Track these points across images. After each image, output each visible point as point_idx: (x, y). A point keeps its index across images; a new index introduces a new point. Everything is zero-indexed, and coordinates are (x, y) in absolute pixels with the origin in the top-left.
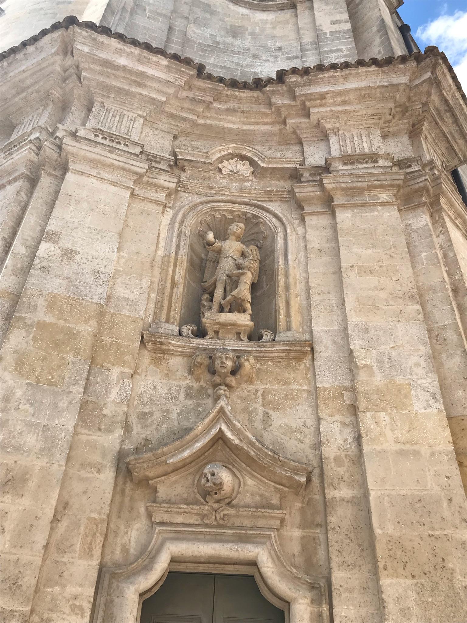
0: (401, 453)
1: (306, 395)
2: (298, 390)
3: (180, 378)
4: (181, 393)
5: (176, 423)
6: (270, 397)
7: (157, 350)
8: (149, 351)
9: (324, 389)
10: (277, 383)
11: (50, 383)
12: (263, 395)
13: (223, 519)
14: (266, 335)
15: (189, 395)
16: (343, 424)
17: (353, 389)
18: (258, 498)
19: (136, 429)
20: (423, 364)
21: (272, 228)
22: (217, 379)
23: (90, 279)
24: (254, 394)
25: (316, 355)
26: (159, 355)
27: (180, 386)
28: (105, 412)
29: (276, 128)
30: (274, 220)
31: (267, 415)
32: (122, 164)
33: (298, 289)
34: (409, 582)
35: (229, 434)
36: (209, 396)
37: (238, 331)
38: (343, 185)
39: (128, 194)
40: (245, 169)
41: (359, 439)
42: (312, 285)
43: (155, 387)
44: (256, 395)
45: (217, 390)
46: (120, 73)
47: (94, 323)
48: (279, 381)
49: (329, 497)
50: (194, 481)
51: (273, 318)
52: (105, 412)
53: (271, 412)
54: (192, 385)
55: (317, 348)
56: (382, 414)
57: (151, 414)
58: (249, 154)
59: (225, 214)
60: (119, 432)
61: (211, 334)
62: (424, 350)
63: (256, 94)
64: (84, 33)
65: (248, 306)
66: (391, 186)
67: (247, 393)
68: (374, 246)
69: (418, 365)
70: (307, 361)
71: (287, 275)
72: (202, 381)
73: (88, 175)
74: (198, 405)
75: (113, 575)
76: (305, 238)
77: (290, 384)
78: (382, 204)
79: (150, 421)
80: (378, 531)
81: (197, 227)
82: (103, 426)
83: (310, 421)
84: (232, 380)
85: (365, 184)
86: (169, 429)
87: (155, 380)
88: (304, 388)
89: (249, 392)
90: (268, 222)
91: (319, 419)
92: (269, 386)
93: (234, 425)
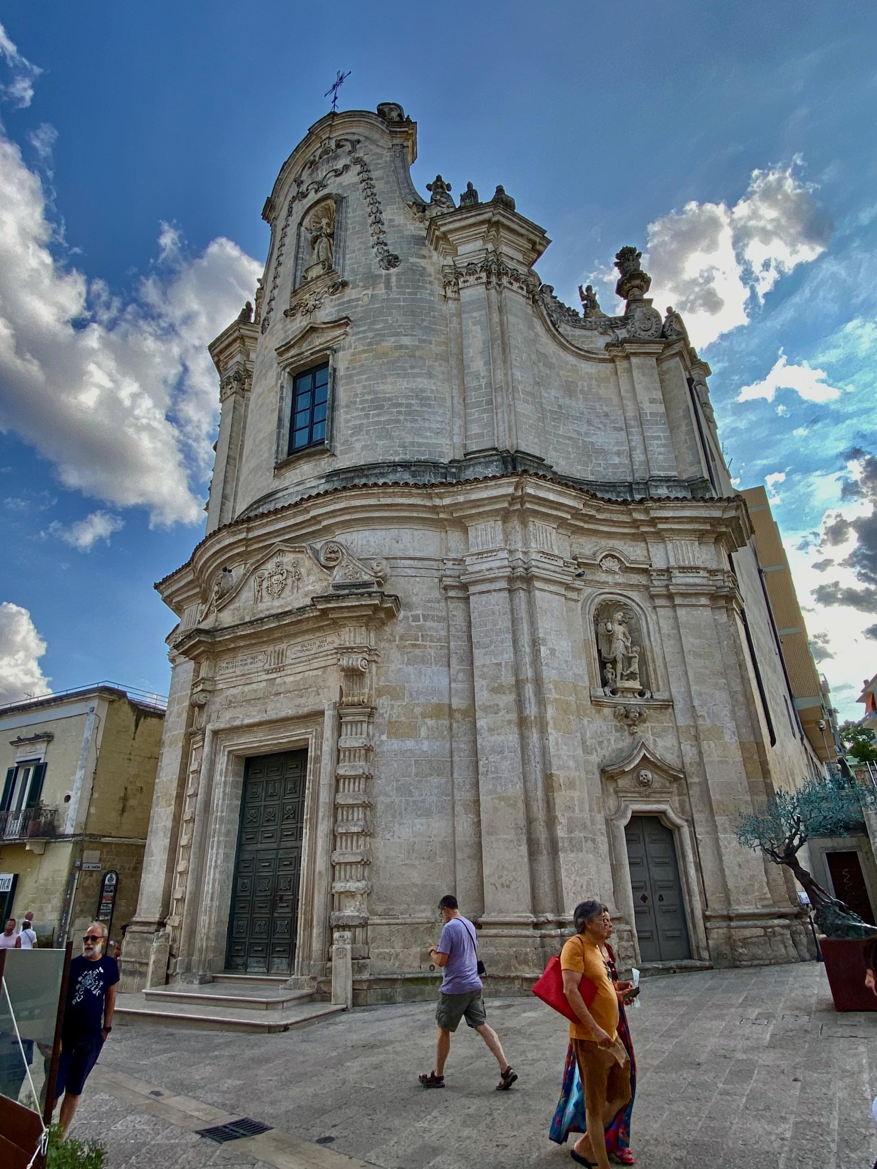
0: (721, 762)
15: (617, 731)
16: (692, 746)
17: (696, 727)
20: (729, 715)
22: (630, 722)
23: (564, 665)
30: (638, 609)
31: (655, 740)
33: (659, 662)
41: (700, 753)
42: (667, 660)
46: (548, 503)
47: (574, 695)
48: (658, 721)
52: (588, 743)
55: (676, 702)
57: (602, 741)
58: (617, 555)
60: (595, 754)
62: (729, 707)
63: (622, 508)
68: (700, 638)
69: (726, 715)
70: (670, 710)
71: (652, 652)
73: (545, 591)
74: (622, 736)
75: (612, 820)
76: (658, 623)
83: (675, 743)
91: (680, 743)
92: (653, 724)
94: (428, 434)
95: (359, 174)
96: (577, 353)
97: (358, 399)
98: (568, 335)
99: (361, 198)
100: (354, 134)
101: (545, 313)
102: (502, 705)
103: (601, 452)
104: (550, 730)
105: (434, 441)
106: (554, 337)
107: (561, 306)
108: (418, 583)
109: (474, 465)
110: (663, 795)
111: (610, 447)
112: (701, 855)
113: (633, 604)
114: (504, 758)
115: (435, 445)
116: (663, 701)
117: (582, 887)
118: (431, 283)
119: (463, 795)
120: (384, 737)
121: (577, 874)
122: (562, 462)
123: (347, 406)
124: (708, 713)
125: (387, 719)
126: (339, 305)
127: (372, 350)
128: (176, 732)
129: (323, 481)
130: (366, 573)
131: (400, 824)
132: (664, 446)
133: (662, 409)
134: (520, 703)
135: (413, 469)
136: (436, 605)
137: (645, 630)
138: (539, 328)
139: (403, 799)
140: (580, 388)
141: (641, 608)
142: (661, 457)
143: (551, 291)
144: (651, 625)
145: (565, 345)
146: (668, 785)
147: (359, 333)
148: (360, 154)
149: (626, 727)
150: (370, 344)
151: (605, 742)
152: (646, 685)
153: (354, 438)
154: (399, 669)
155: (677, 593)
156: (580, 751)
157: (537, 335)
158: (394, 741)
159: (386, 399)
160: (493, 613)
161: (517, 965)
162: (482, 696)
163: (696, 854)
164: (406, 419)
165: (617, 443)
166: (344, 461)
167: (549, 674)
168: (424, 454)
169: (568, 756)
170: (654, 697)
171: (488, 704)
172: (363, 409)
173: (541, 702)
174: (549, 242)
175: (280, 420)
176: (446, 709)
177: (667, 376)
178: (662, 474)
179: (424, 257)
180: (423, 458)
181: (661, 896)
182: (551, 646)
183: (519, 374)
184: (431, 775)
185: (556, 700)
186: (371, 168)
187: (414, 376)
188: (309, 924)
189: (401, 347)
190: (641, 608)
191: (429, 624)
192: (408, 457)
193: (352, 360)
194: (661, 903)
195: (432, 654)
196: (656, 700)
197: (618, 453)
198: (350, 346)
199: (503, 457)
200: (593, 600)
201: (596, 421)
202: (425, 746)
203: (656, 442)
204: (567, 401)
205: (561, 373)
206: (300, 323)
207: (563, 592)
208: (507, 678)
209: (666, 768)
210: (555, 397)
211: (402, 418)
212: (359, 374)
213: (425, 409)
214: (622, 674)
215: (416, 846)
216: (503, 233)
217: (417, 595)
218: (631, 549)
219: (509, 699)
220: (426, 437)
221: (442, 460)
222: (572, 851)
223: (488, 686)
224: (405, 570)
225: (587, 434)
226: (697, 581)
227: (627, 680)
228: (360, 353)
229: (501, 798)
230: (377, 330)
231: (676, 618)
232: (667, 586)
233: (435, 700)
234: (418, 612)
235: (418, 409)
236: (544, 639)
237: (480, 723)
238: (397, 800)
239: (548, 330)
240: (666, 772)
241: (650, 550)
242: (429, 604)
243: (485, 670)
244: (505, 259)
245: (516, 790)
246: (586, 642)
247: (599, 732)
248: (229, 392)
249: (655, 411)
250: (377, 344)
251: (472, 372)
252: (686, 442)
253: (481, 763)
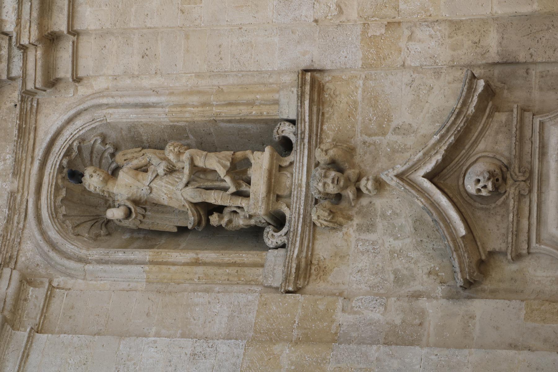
1: (371, 82)
2: (364, 91)
3: (346, 240)
4: (366, 238)
5: (408, 241)
6: (373, 126)
7: (306, 274)
8: (307, 284)
10: (354, 118)
12: (370, 135)
13: (524, 172)
14: (282, 131)
15: (370, 228)
16: (410, 38)
18: (500, 137)
19: (416, 287)
21: (93, 126)
24: (369, 146)
25: (316, 66)
26: (313, 271)
27: (358, 240)
28: (398, 321)
30: (78, 123)
31: (397, 130)
35: (429, 167)
36: (371, 203)
37: (278, 169)
38: (35, 14)
39: (42, 338)
43: (358, 271)
44: (370, 144)
45: (367, 189)
47: (277, 348)
49: (497, 59)
50: (482, 209)
51: (249, 126)
52: (398, 321)
53: (393, 125)
54: (355, 226)
57: (396, 272)
59: (60, 198)
60: (423, 303)
65: (239, 154)
67: (368, 155)
72: (350, 213)
74: (384, 216)
77: (355, 102)
79: (405, 272)
81: (85, 241)
82: (417, 321)
84: (352, 173)
87: (350, 271)
88: (361, 85)
89: (365, 153)
90: (81, 132)
93: (419, 160)
110: (528, 133)
113: (66, 134)
116: (301, 97)
146: (501, 117)
149: (364, 201)
151: (398, 264)
155: (41, 26)
170: (293, 117)
190: (78, 114)
196: (300, 113)
200: (53, 246)
207: (22, 335)
209: (461, 123)
227: (249, 182)
231: (103, 34)
232: (23, 48)
240: (471, 122)
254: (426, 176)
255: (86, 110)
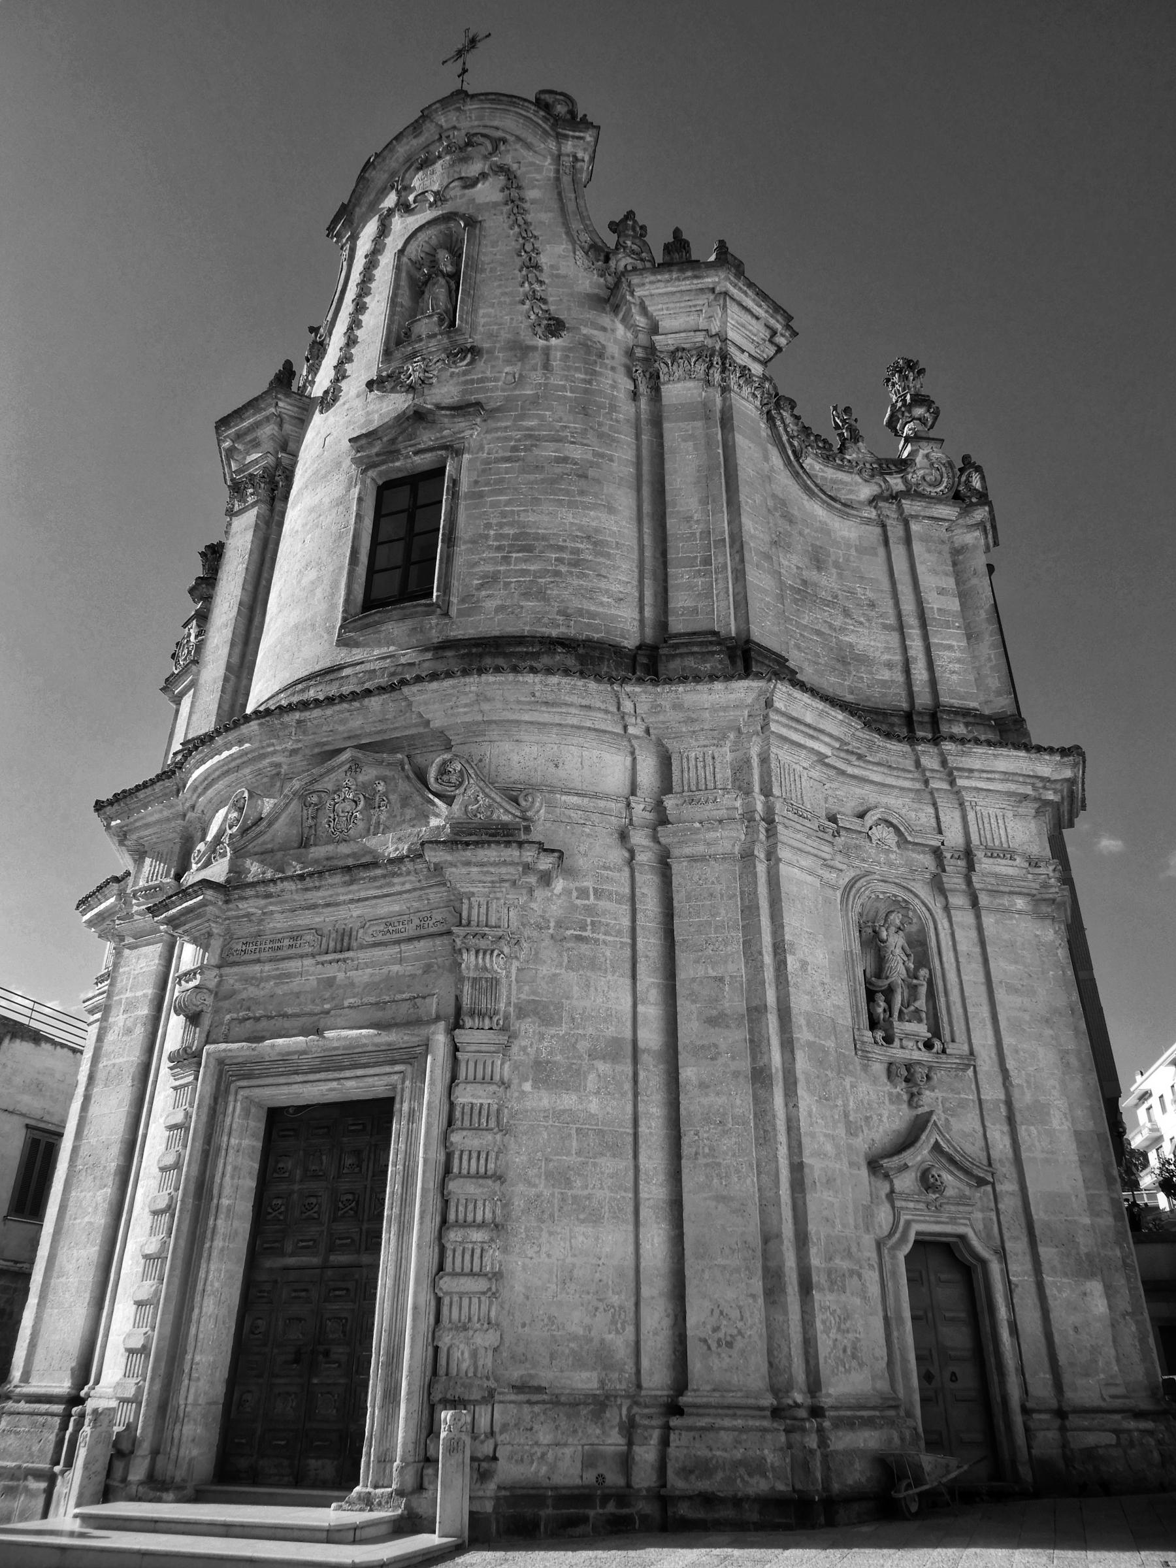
0: (1047, 1161)
9: (987, 1101)
11: (826, 1099)
15: (892, 1102)
16: (1003, 1132)
29: (918, 786)
32: (816, 852)
34: (1055, 1250)
39: (817, 883)
40: (891, 838)
47: (833, 1038)
48: (952, 1090)
52: (851, 1118)
56: (1032, 1128)
58: (895, 821)
61: (897, 1043)
64: (784, 689)
66: (1028, 894)
68: (1016, 962)
69: (1054, 1087)
78: (1019, 912)
80: (1035, 1217)
85: (1007, 889)
86: (885, 1131)
94: (605, 599)
95: (502, 190)
96: (828, 504)
97: (492, 532)
98: (816, 476)
99: (506, 226)
100: (497, 128)
101: (785, 438)
102: (723, 1046)
103: (863, 660)
104: (800, 1092)
105: (613, 611)
106: (796, 475)
107: (806, 430)
108: (588, 835)
109: (681, 655)
111: (878, 654)
112: (1017, 1309)
113: (917, 901)
114: (725, 1132)
115: (614, 618)
117: (845, 1351)
118: (613, 369)
119: (655, 1191)
120: (527, 1086)
121: (839, 1329)
122: (805, 665)
123: (473, 542)
124: (1028, 1082)
125: (532, 1057)
126: (466, 383)
127: (518, 459)
128: (121, 1060)
129: (429, 655)
130: (506, 810)
131: (551, 1234)
132: (959, 661)
133: (954, 605)
134: (756, 1045)
135: (581, 651)
136: (616, 875)
137: (933, 944)
138: (776, 460)
139: (557, 1191)
140: (833, 558)
141: (929, 910)
142: (955, 677)
143: (793, 408)
144: (942, 936)
145: (813, 488)
147: (497, 429)
148: (508, 160)
150: (515, 449)
151: (875, 1117)
152: (936, 1031)
153: (483, 593)
154: (555, 975)
156: (841, 1131)
157: (772, 469)
158: (544, 1094)
159: (537, 537)
160: (711, 895)
161: (746, 1477)
162: (690, 1028)
163: (1011, 1307)
164: (571, 573)
165: (887, 649)
166: (465, 628)
167: (800, 1003)
168: (597, 631)
169: (826, 1135)
170: (948, 1051)
171: (699, 1043)
172: (499, 548)
173: (788, 1045)
174: (795, 334)
175: (354, 553)
176: (629, 1048)
177: (961, 557)
178: (956, 702)
179: (604, 329)
180: (596, 636)
181: (953, 1374)
182: (802, 956)
183: (750, 523)
184: (602, 1154)
185: (810, 1045)
186: (524, 183)
187: (586, 507)
188: (391, 1396)
189: (565, 460)
190: (929, 910)
191: (603, 904)
192: (572, 632)
193: (484, 471)
194: (953, 1385)
195: (608, 954)
197: (889, 665)
198: (481, 448)
199: (728, 648)
201: (857, 613)
202: (594, 1106)
203: (946, 653)
204: (812, 575)
205: (807, 531)
206: (396, 403)
208: (733, 1002)
210: (798, 568)
211: (563, 569)
212: (495, 492)
213: (601, 560)
214: (901, 1012)
215: (575, 1272)
216: (733, 309)
217: (586, 855)
218: (913, 814)
219: (738, 1035)
220: (602, 604)
221: (626, 643)
222: (831, 1291)
223: (700, 1013)
224: (567, 811)
225: (842, 630)
226: (1011, 871)
228: (497, 461)
229: (721, 1199)
230: (528, 429)
233: (611, 1031)
234: (585, 884)
235: (590, 558)
236: (792, 944)
237: (688, 1073)
238: (547, 1193)
239: (788, 463)
241: (942, 819)
242: (605, 873)
243: (695, 986)
244: (732, 350)
245: (746, 1185)
246: (849, 955)
247: (865, 1102)
248: (250, 500)
249: (944, 607)
250: (525, 450)
251: (678, 512)
252: (990, 659)
253: (685, 1141)
254: (937, 1142)
255: (931, 914)
